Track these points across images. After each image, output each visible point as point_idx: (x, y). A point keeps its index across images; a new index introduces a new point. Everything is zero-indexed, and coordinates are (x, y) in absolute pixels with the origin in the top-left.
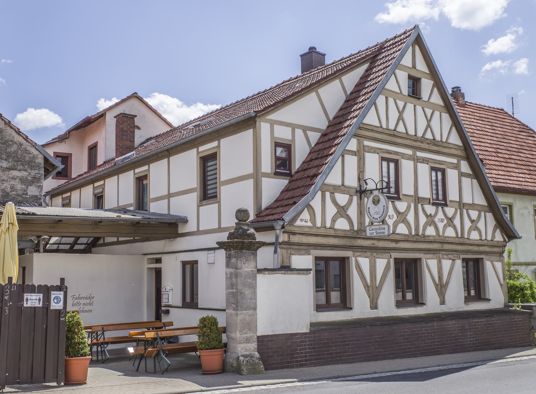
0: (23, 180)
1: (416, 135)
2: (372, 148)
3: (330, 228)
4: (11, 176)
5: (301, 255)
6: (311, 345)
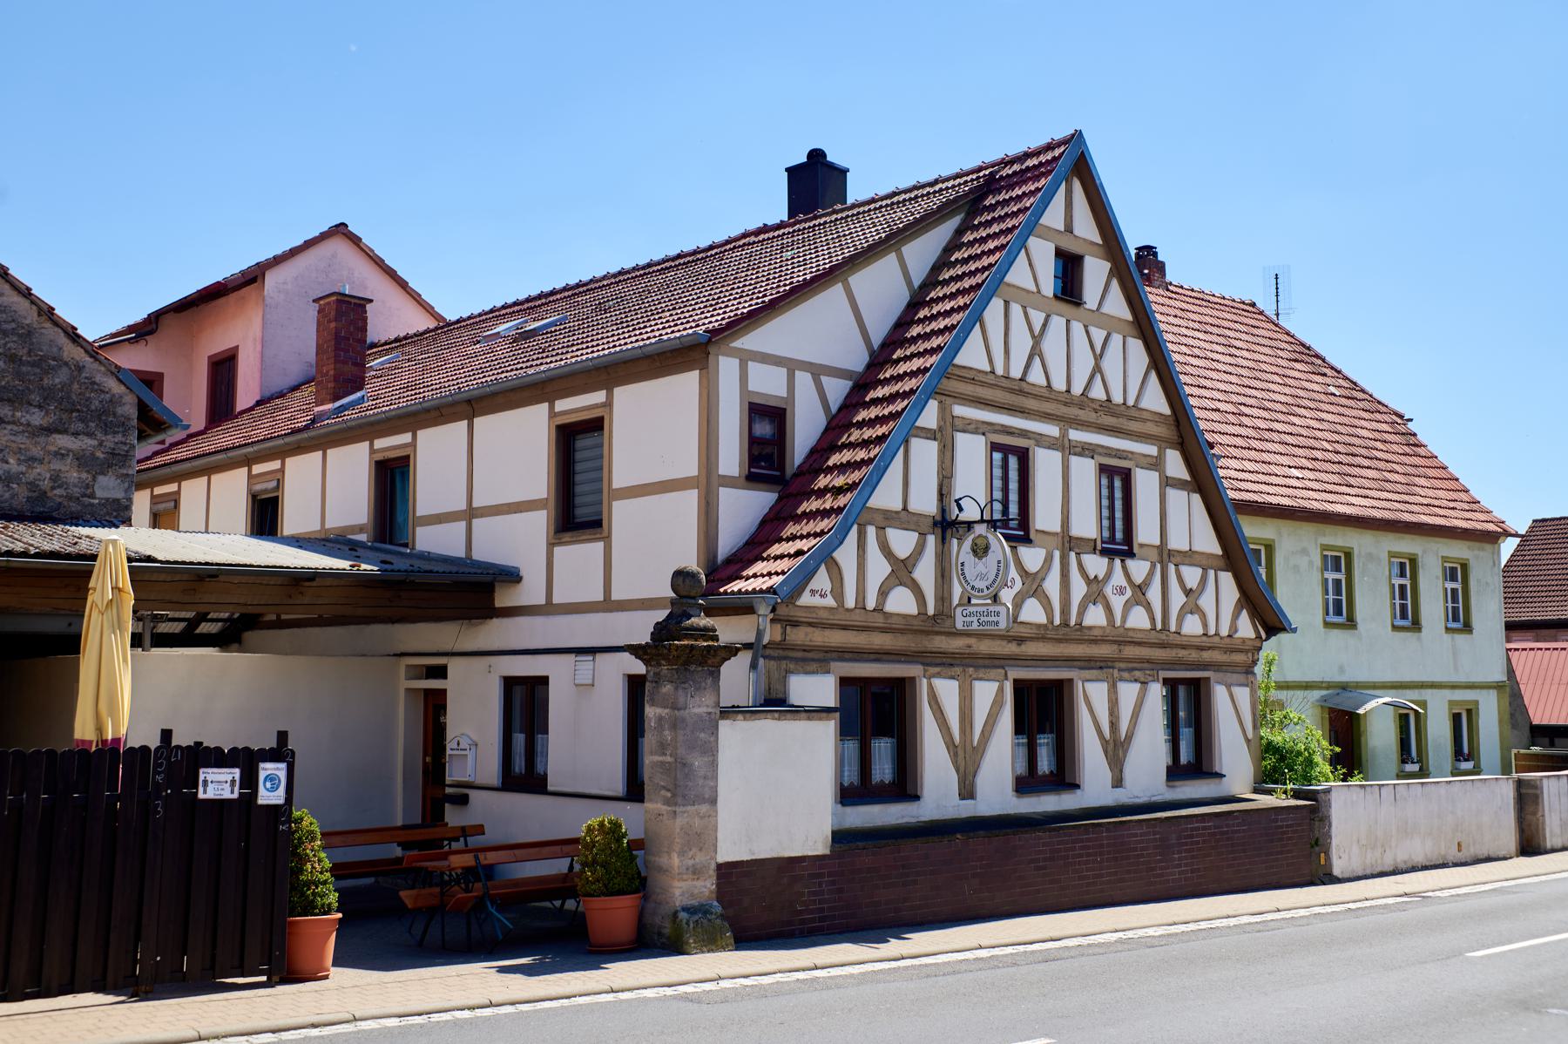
0: (83, 460)
1: (1068, 391)
2: (970, 422)
4: (53, 448)
6: (833, 883)
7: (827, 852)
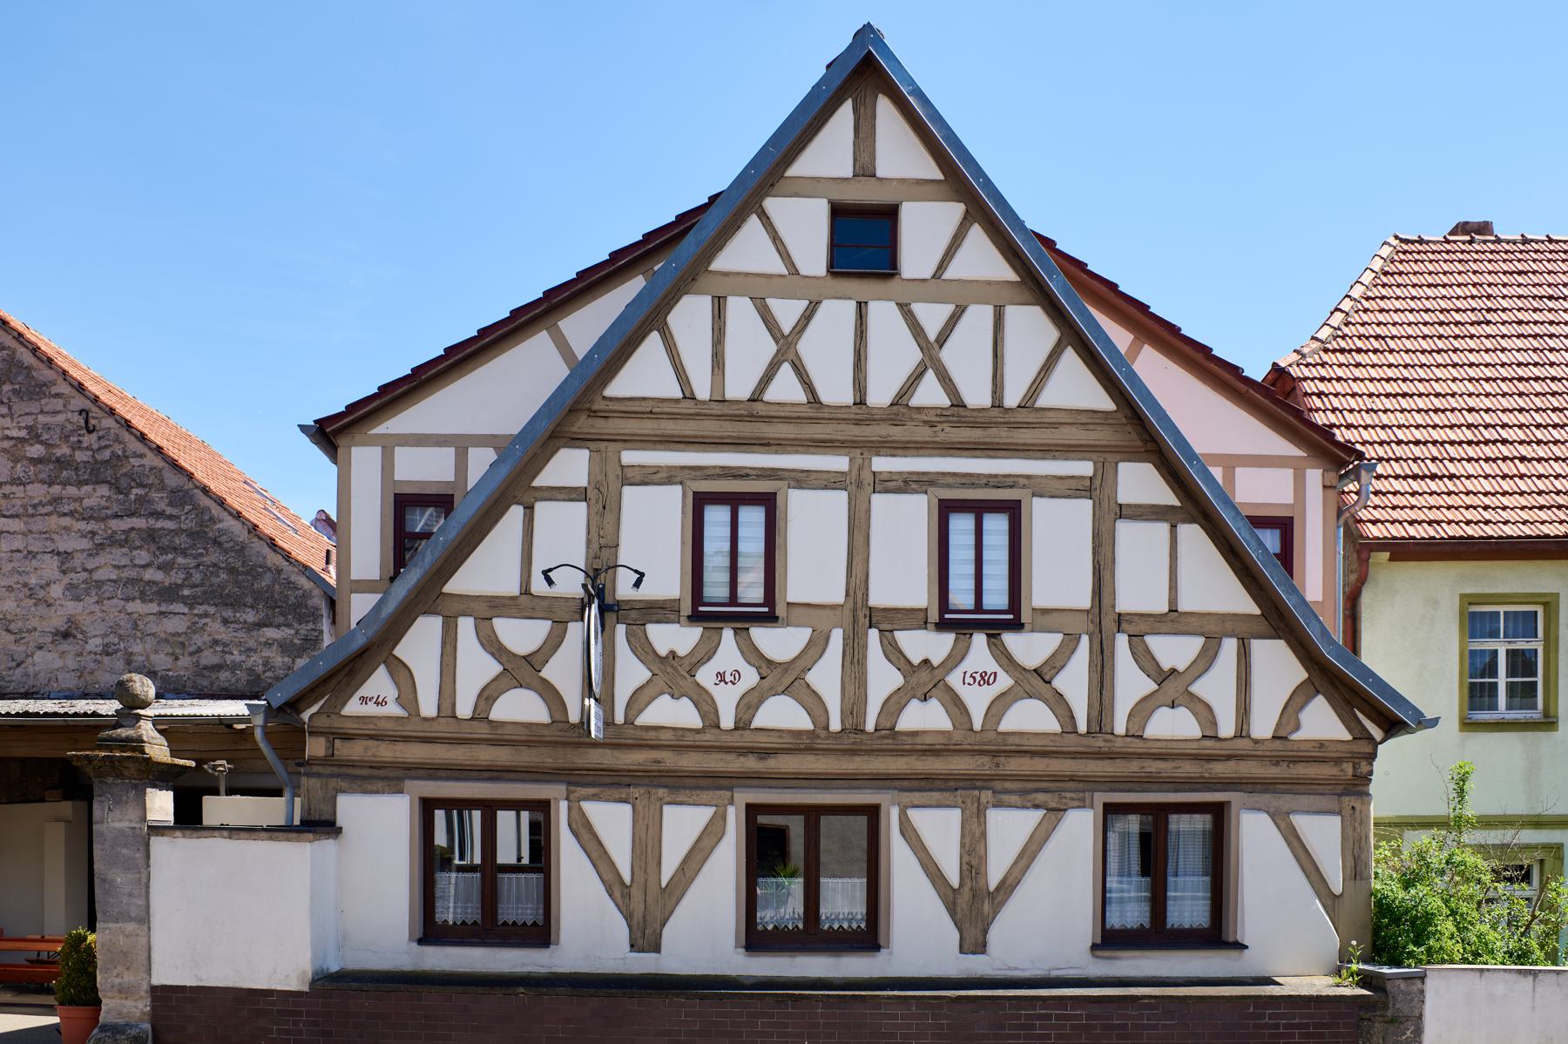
0: (285, 647)
5: (371, 792)
7: (306, 988)
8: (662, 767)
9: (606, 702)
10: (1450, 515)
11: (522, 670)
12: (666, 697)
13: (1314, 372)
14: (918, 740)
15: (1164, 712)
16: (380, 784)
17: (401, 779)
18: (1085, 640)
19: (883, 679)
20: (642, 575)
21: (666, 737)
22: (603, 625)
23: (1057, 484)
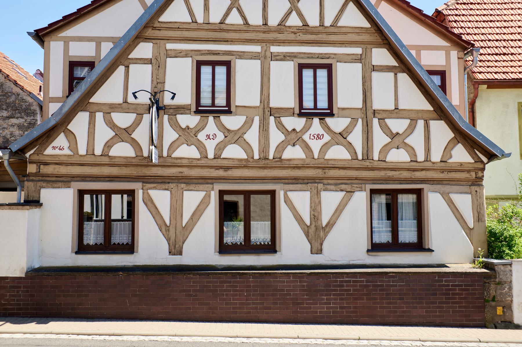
0: (20, 127)
1: (266, 24)
2: (181, 51)
3: (101, 155)
4: (10, 124)
5: (56, 188)
6: (27, 291)
8: (183, 175)
9: (159, 147)
10: (512, 70)
11: (123, 134)
12: (185, 145)
13: (453, 12)
14: (291, 163)
15: (394, 150)
16: (60, 184)
17: (70, 182)
18: (360, 121)
19: (276, 137)
20: (175, 94)
21: (185, 162)
22: (158, 116)
23: (347, 57)
